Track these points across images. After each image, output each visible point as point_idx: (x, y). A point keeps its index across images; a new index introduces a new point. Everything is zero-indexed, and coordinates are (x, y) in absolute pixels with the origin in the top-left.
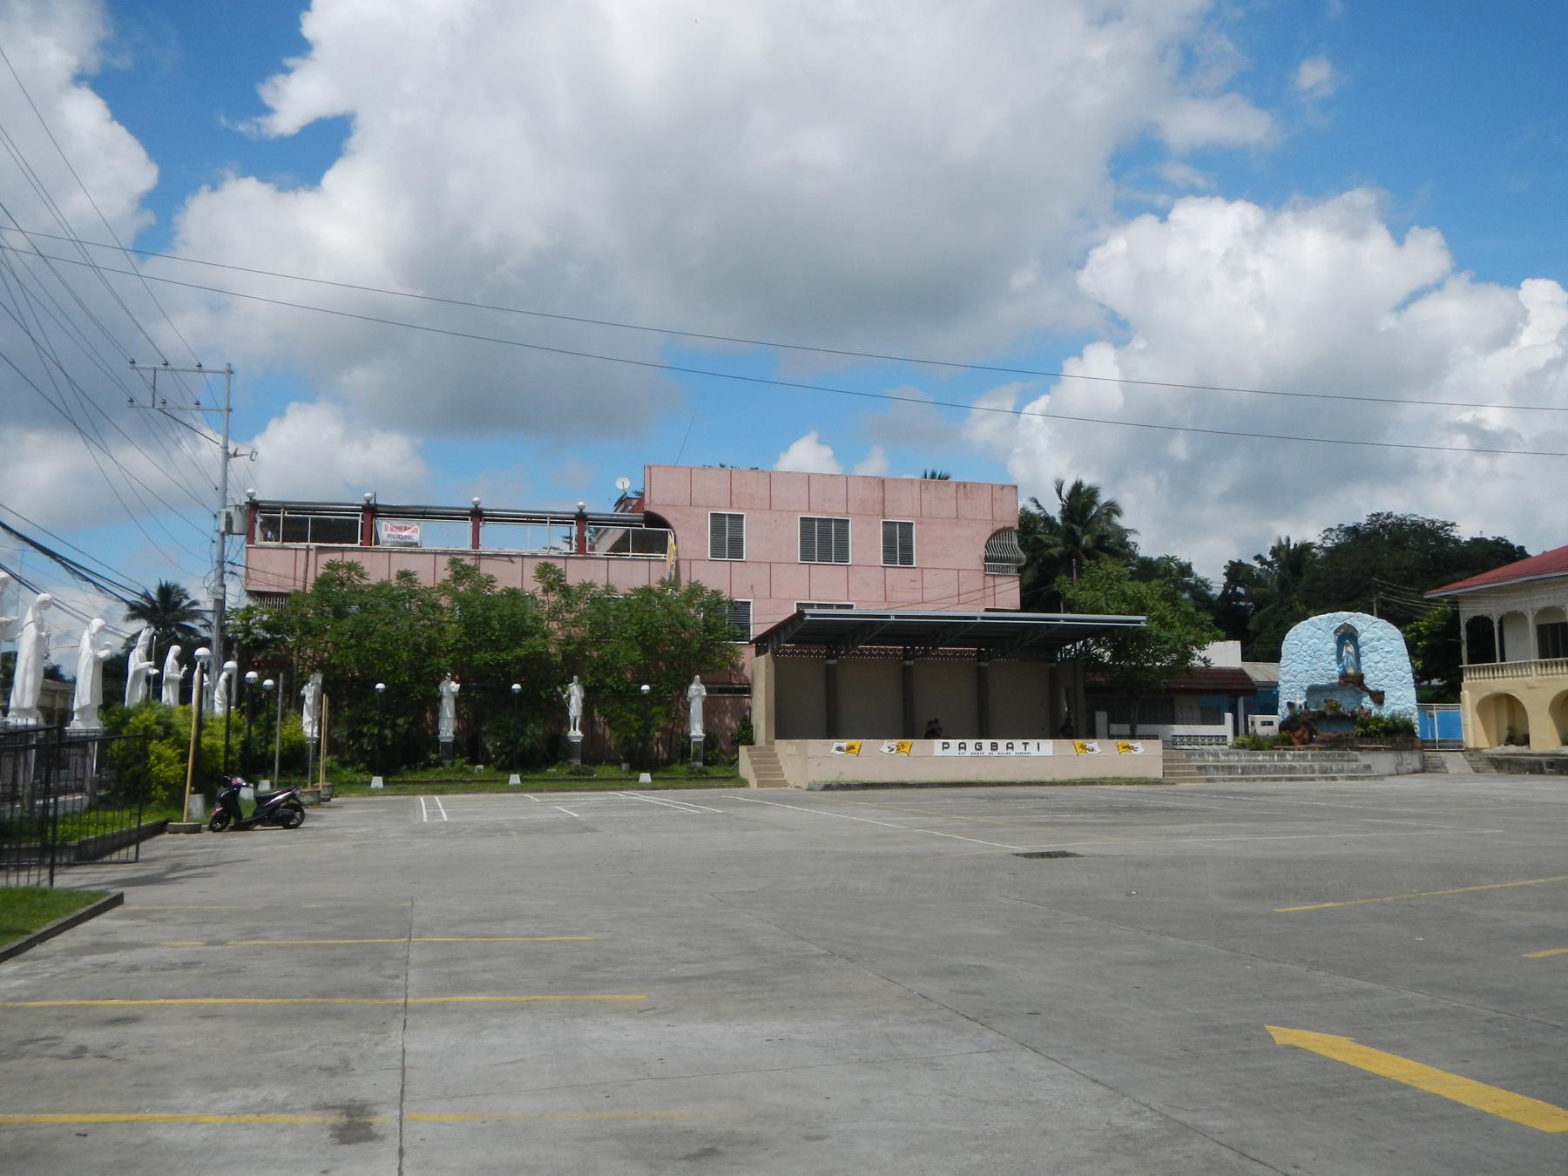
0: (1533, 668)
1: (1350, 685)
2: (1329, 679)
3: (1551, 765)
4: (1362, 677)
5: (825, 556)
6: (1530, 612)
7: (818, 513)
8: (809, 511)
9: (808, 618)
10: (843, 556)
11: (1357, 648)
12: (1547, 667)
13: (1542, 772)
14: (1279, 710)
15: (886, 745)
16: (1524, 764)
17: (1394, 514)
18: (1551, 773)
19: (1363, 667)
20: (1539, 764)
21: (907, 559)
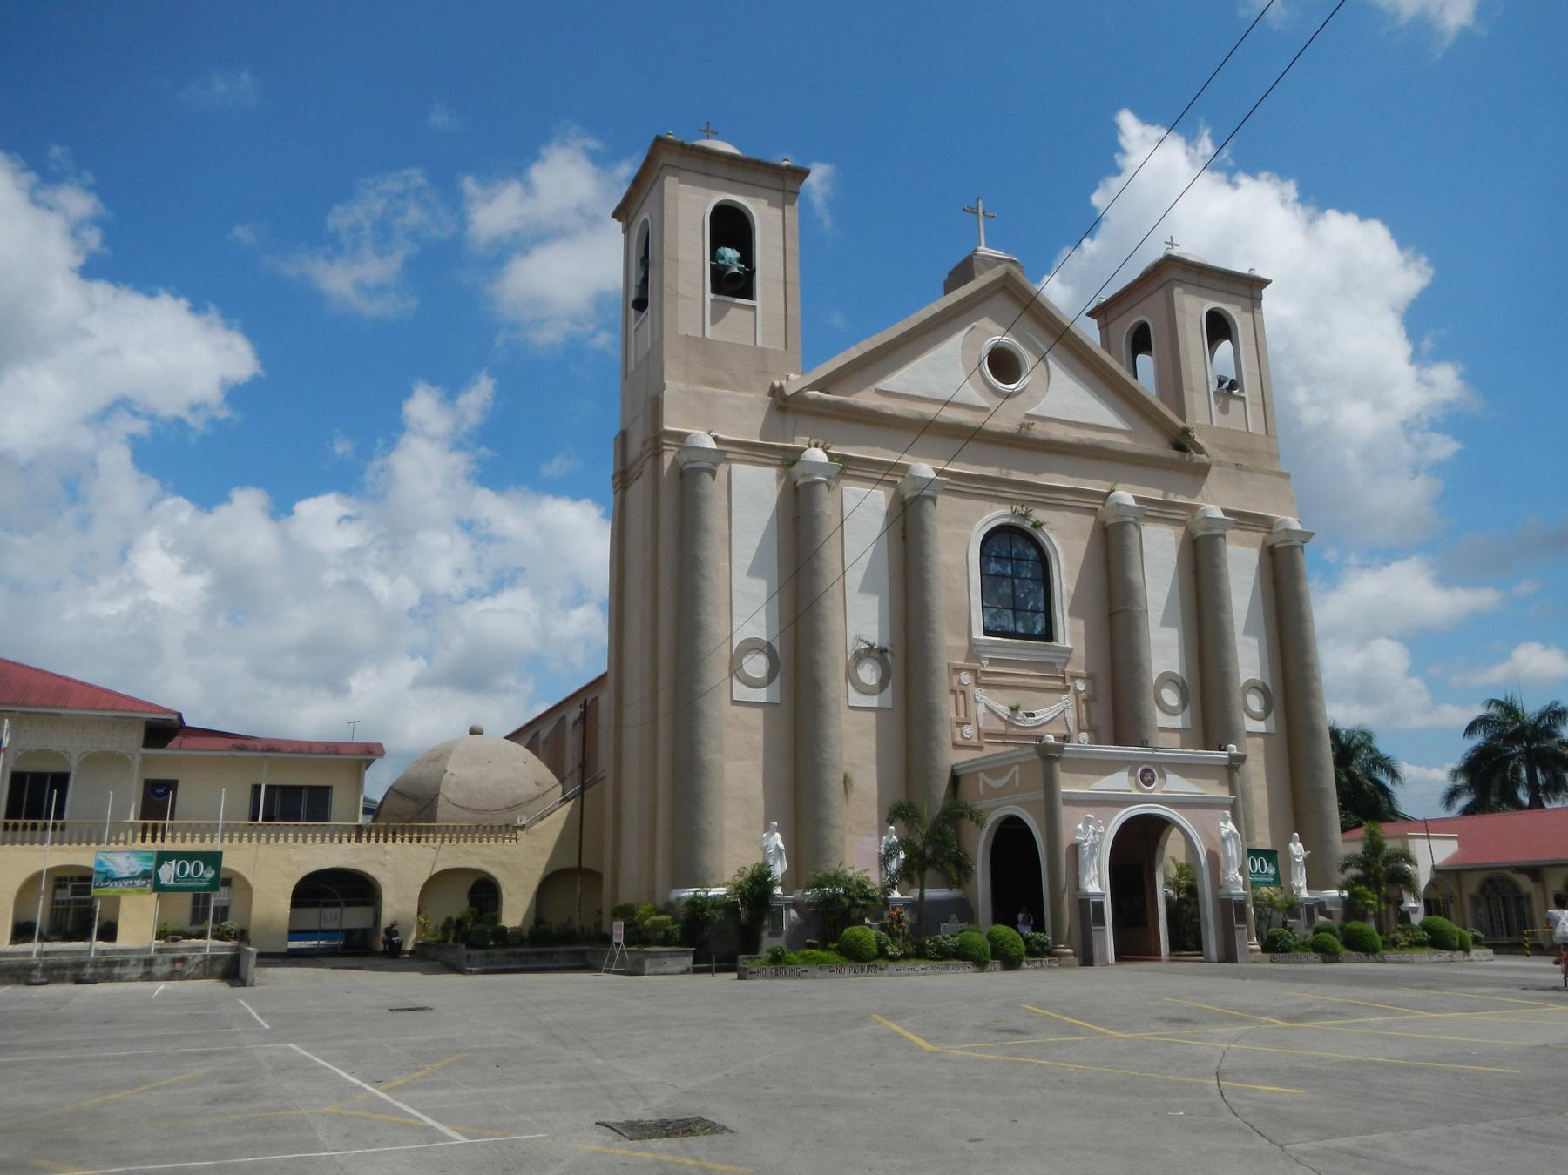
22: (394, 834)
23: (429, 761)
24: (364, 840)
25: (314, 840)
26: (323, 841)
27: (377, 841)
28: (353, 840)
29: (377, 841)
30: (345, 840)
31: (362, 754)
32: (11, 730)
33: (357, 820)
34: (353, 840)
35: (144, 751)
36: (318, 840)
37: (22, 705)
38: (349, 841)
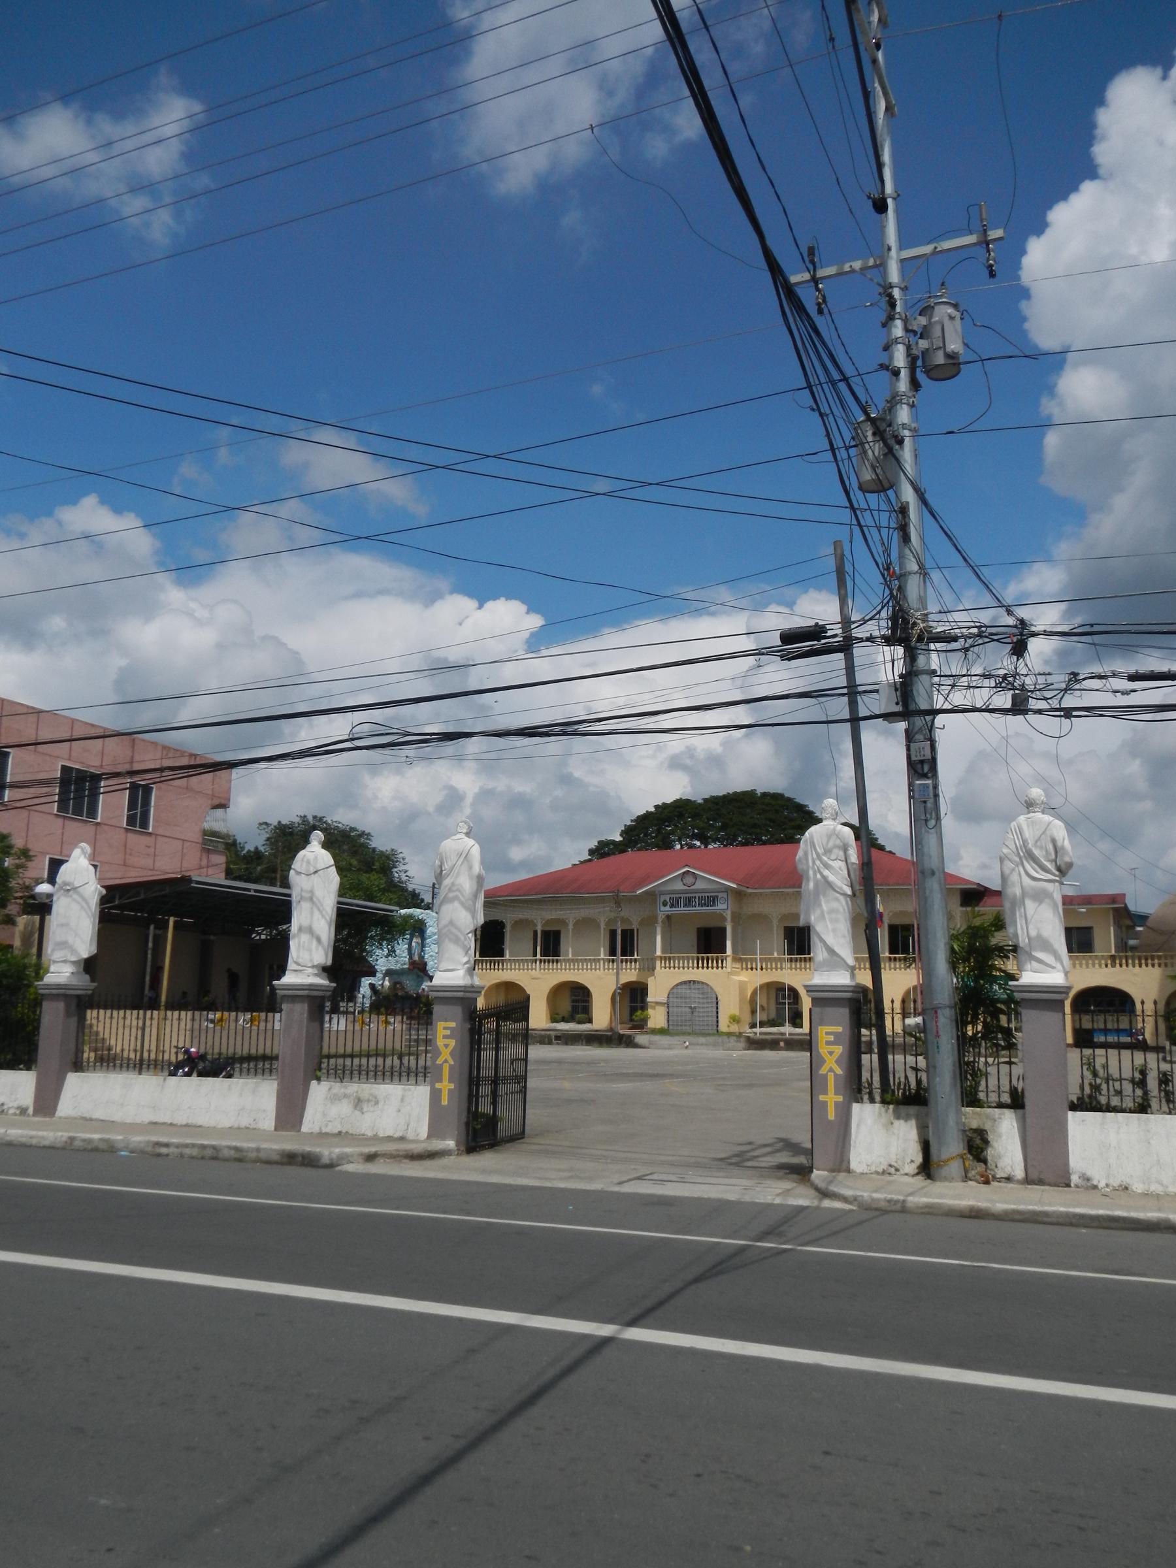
0: (538, 962)
1: (416, 970)
2: (402, 965)
3: (557, 1038)
4: (425, 964)
5: (78, 811)
6: (539, 921)
7: (75, 762)
8: (70, 760)
9: (194, 885)
10: (92, 813)
11: (423, 939)
12: (545, 963)
13: (550, 1043)
14: (361, 989)
15: (243, 1018)
16: (535, 1037)
17: (325, 819)
18: (558, 1044)
19: (426, 956)
20: (549, 1037)
21: (144, 824)
22: (1146, 960)
23: (1171, 904)
24: (1118, 965)
25: (1081, 966)
26: (1087, 967)
27: (1127, 966)
28: (1109, 966)
29: (1127, 966)
30: (1103, 966)
31: (1107, 904)
32: (882, 901)
33: (1110, 952)
34: (1109, 966)
35: (961, 909)
36: (1084, 966)
37: (886, 885)
38: (1106, 966)
